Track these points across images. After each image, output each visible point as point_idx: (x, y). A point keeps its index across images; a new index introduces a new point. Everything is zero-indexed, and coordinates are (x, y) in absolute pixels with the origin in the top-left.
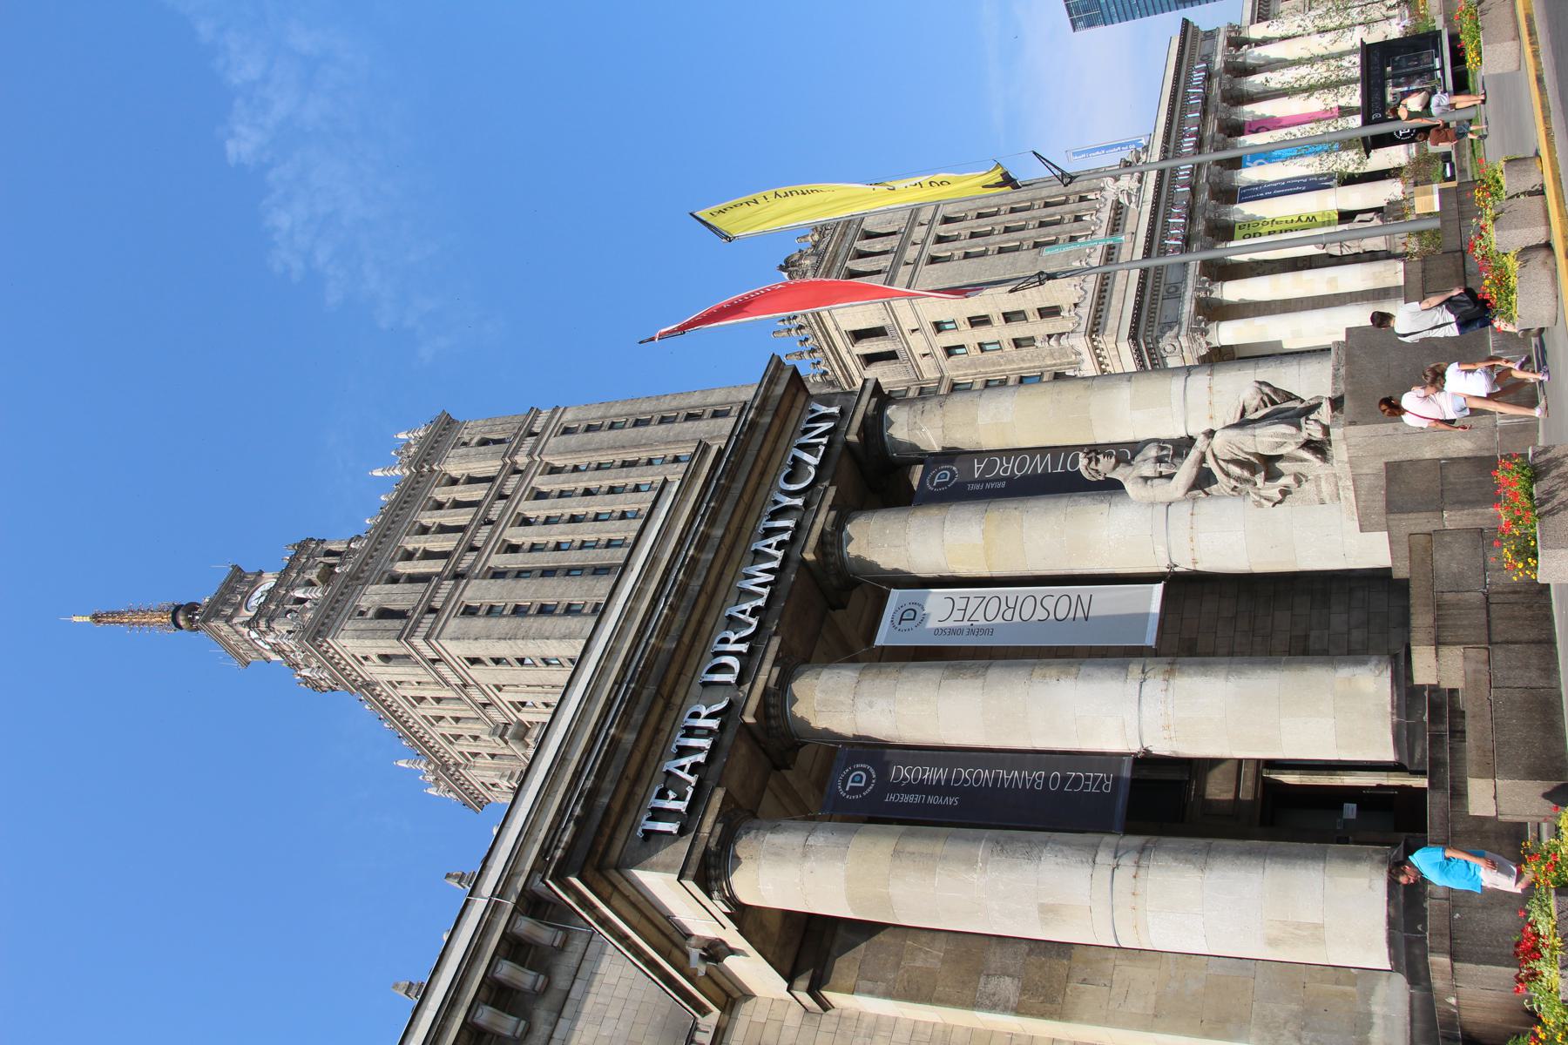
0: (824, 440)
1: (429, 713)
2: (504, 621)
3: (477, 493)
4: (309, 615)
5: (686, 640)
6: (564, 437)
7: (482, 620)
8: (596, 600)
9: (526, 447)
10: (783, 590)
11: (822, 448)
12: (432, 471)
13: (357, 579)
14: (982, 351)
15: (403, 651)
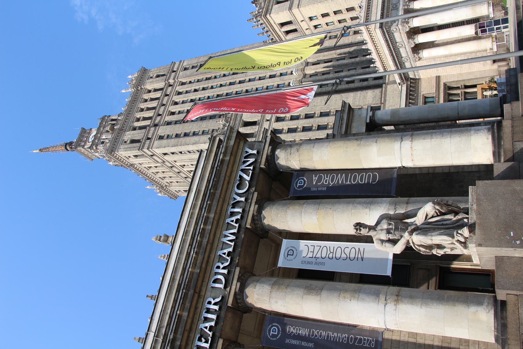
0: (251, 168)
1: (154, 171)
2: (173, 140)
3: (158, 95)
4: (108, 145)
5: (204, 266)
6: (185, 72)
7: (166, 140)
8: (203, 129)
9: (172, 77)
10: (239, 243)
11: (251, 172)
12: (141, 88)
13: (122, 130)
14: (327, 25)
15: (141, 154)
